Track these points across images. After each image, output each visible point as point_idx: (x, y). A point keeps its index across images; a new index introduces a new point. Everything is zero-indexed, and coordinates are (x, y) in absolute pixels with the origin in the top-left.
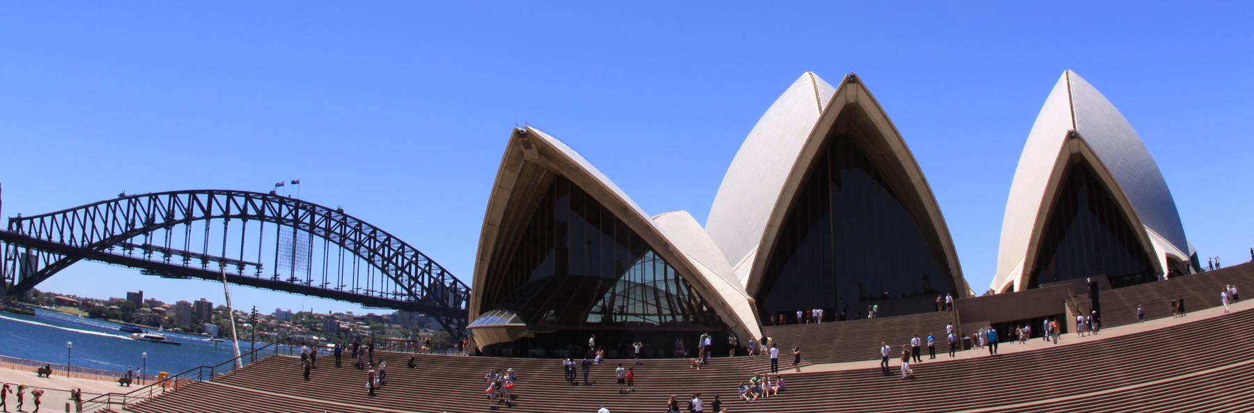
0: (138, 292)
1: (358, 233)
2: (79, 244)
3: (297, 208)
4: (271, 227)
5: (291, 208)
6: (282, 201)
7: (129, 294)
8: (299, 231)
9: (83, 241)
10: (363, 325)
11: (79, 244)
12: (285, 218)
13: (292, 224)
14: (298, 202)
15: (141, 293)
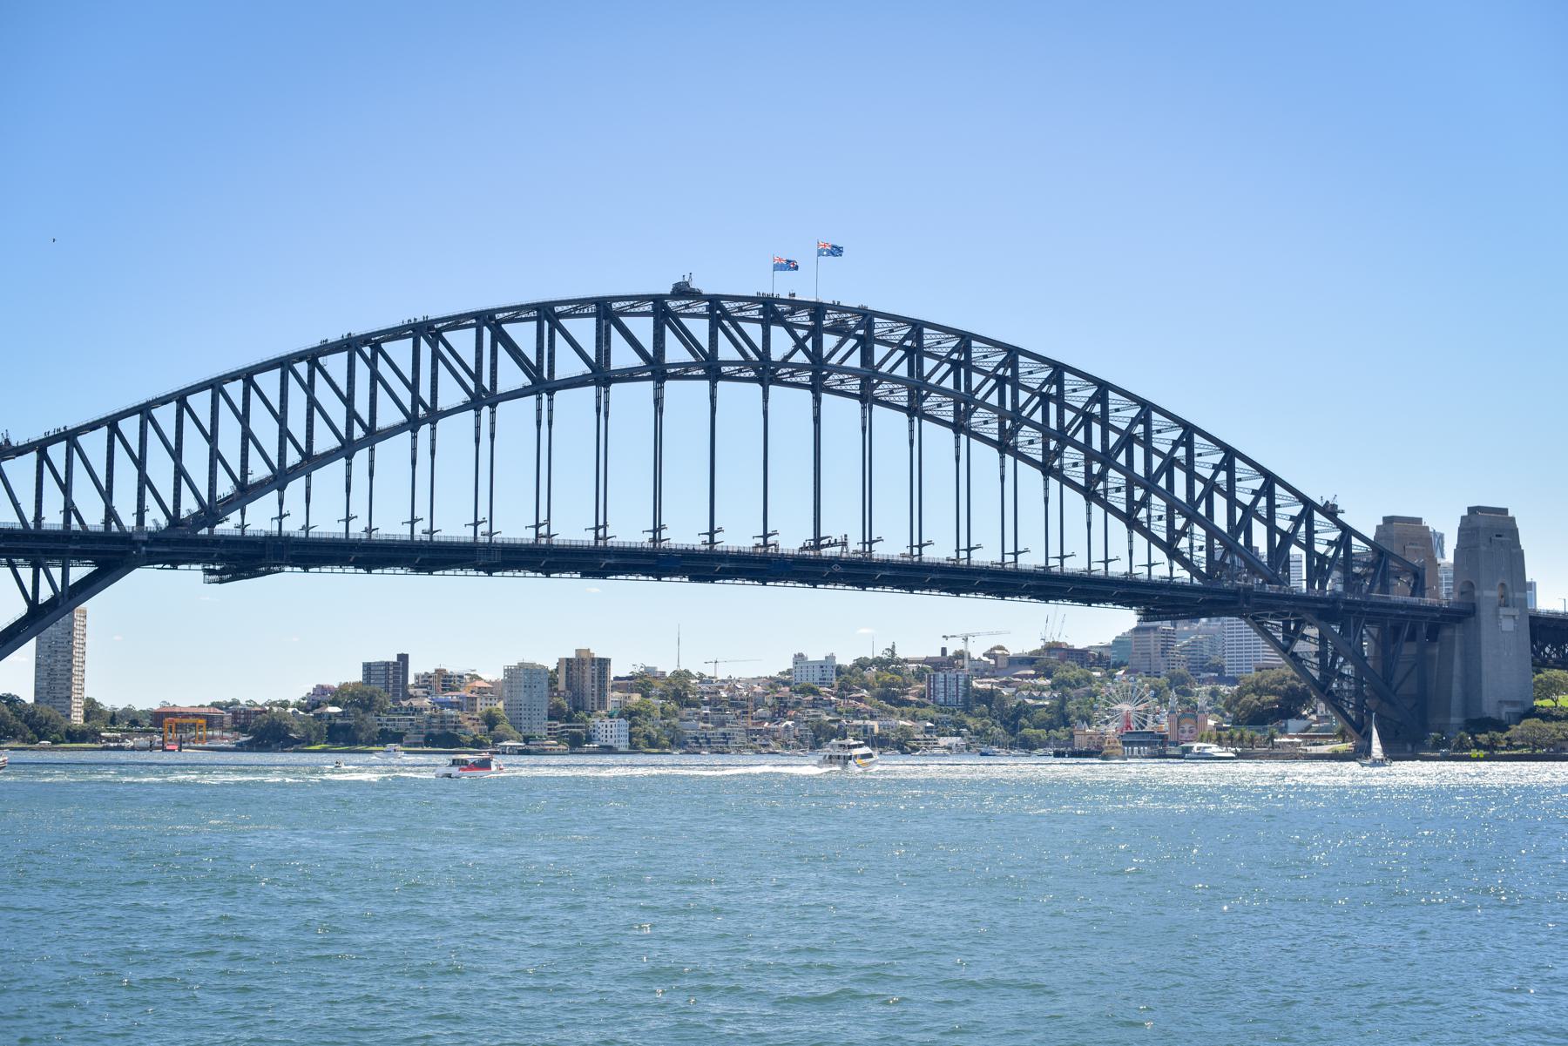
0: (395, 660)
1: (1008, 388)
2: (129, 522)
3: (816, 332)
4: (740, 397)
5: (801, 333)
6: (772, 311)
7: (368, 668)
8: (825, 397)
9: (141, 512)
10: (1033, 677)
11: (129, 522)
12: (785, 362)
13: (805, 378)
14: (818, 310)
15: (403, 658)
